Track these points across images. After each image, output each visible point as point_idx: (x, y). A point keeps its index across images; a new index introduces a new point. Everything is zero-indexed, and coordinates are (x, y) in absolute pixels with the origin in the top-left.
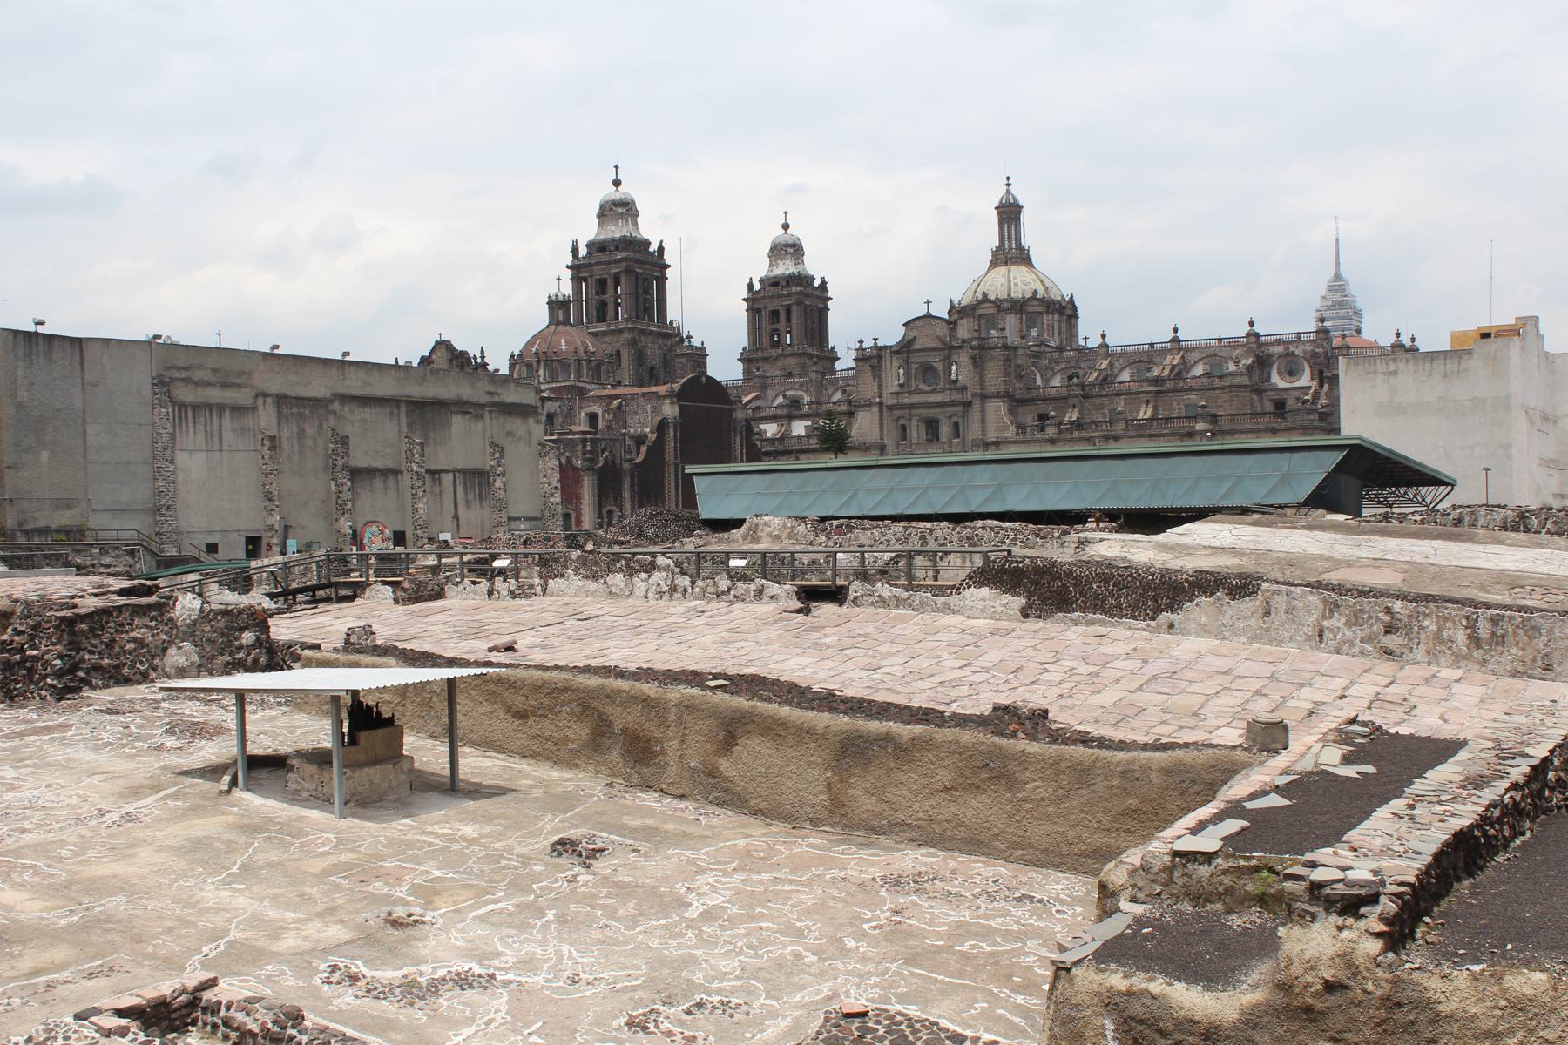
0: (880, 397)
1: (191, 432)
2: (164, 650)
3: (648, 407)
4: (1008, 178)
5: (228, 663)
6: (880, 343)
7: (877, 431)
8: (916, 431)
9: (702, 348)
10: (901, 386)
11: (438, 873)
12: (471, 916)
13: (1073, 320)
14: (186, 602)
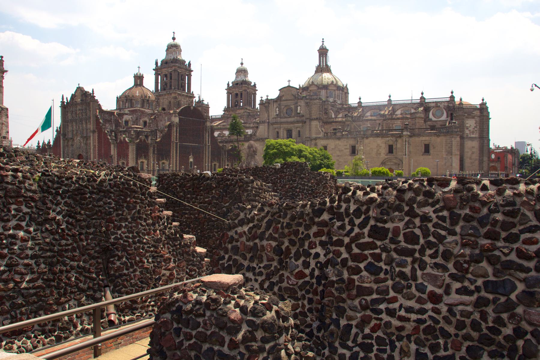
0: (268, 120)
3: (166, 118)
4: (323, 39)
6: (269, 98)
7: (266, 133)
8: (283, 133)
9: (208, 105)
10: (277, 115)
13: (347, 94)
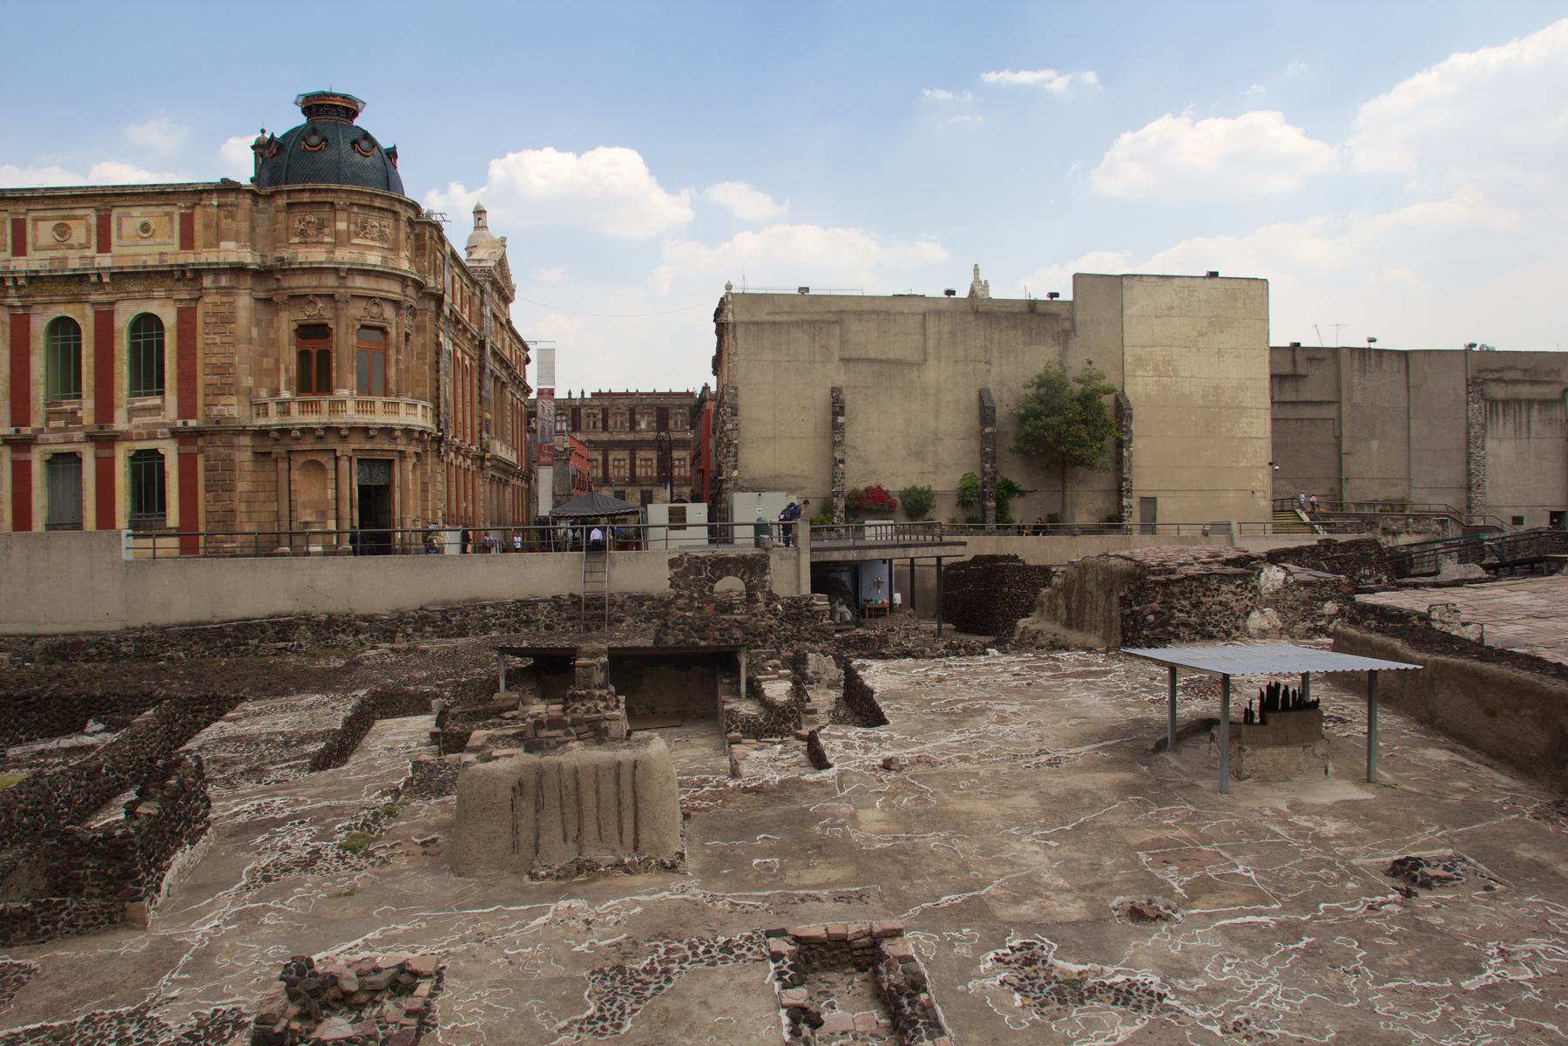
1: (1501, 421)
2: (1248, 614)
5: (1310, 629)
11: (1240, 870)
12: (1217, 924)
14: (1271, 574)
